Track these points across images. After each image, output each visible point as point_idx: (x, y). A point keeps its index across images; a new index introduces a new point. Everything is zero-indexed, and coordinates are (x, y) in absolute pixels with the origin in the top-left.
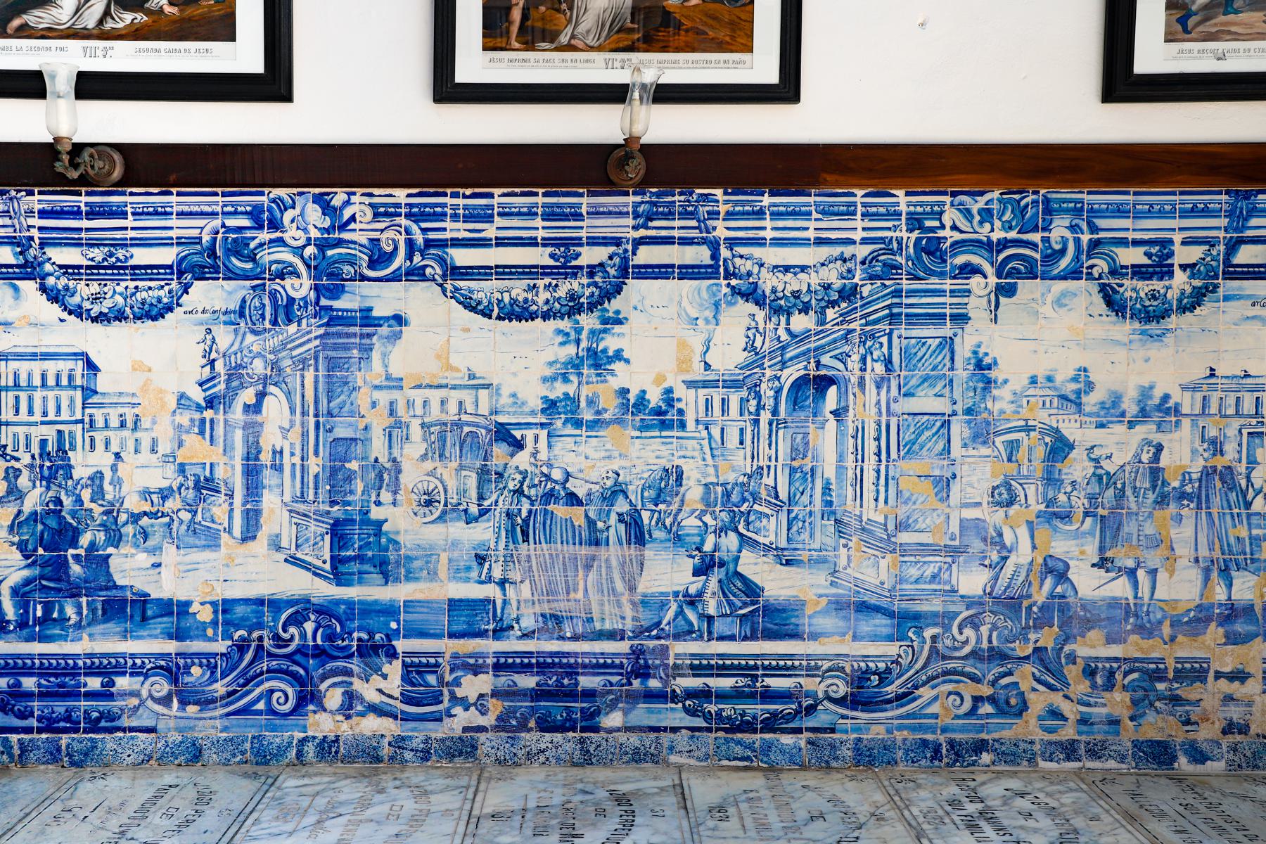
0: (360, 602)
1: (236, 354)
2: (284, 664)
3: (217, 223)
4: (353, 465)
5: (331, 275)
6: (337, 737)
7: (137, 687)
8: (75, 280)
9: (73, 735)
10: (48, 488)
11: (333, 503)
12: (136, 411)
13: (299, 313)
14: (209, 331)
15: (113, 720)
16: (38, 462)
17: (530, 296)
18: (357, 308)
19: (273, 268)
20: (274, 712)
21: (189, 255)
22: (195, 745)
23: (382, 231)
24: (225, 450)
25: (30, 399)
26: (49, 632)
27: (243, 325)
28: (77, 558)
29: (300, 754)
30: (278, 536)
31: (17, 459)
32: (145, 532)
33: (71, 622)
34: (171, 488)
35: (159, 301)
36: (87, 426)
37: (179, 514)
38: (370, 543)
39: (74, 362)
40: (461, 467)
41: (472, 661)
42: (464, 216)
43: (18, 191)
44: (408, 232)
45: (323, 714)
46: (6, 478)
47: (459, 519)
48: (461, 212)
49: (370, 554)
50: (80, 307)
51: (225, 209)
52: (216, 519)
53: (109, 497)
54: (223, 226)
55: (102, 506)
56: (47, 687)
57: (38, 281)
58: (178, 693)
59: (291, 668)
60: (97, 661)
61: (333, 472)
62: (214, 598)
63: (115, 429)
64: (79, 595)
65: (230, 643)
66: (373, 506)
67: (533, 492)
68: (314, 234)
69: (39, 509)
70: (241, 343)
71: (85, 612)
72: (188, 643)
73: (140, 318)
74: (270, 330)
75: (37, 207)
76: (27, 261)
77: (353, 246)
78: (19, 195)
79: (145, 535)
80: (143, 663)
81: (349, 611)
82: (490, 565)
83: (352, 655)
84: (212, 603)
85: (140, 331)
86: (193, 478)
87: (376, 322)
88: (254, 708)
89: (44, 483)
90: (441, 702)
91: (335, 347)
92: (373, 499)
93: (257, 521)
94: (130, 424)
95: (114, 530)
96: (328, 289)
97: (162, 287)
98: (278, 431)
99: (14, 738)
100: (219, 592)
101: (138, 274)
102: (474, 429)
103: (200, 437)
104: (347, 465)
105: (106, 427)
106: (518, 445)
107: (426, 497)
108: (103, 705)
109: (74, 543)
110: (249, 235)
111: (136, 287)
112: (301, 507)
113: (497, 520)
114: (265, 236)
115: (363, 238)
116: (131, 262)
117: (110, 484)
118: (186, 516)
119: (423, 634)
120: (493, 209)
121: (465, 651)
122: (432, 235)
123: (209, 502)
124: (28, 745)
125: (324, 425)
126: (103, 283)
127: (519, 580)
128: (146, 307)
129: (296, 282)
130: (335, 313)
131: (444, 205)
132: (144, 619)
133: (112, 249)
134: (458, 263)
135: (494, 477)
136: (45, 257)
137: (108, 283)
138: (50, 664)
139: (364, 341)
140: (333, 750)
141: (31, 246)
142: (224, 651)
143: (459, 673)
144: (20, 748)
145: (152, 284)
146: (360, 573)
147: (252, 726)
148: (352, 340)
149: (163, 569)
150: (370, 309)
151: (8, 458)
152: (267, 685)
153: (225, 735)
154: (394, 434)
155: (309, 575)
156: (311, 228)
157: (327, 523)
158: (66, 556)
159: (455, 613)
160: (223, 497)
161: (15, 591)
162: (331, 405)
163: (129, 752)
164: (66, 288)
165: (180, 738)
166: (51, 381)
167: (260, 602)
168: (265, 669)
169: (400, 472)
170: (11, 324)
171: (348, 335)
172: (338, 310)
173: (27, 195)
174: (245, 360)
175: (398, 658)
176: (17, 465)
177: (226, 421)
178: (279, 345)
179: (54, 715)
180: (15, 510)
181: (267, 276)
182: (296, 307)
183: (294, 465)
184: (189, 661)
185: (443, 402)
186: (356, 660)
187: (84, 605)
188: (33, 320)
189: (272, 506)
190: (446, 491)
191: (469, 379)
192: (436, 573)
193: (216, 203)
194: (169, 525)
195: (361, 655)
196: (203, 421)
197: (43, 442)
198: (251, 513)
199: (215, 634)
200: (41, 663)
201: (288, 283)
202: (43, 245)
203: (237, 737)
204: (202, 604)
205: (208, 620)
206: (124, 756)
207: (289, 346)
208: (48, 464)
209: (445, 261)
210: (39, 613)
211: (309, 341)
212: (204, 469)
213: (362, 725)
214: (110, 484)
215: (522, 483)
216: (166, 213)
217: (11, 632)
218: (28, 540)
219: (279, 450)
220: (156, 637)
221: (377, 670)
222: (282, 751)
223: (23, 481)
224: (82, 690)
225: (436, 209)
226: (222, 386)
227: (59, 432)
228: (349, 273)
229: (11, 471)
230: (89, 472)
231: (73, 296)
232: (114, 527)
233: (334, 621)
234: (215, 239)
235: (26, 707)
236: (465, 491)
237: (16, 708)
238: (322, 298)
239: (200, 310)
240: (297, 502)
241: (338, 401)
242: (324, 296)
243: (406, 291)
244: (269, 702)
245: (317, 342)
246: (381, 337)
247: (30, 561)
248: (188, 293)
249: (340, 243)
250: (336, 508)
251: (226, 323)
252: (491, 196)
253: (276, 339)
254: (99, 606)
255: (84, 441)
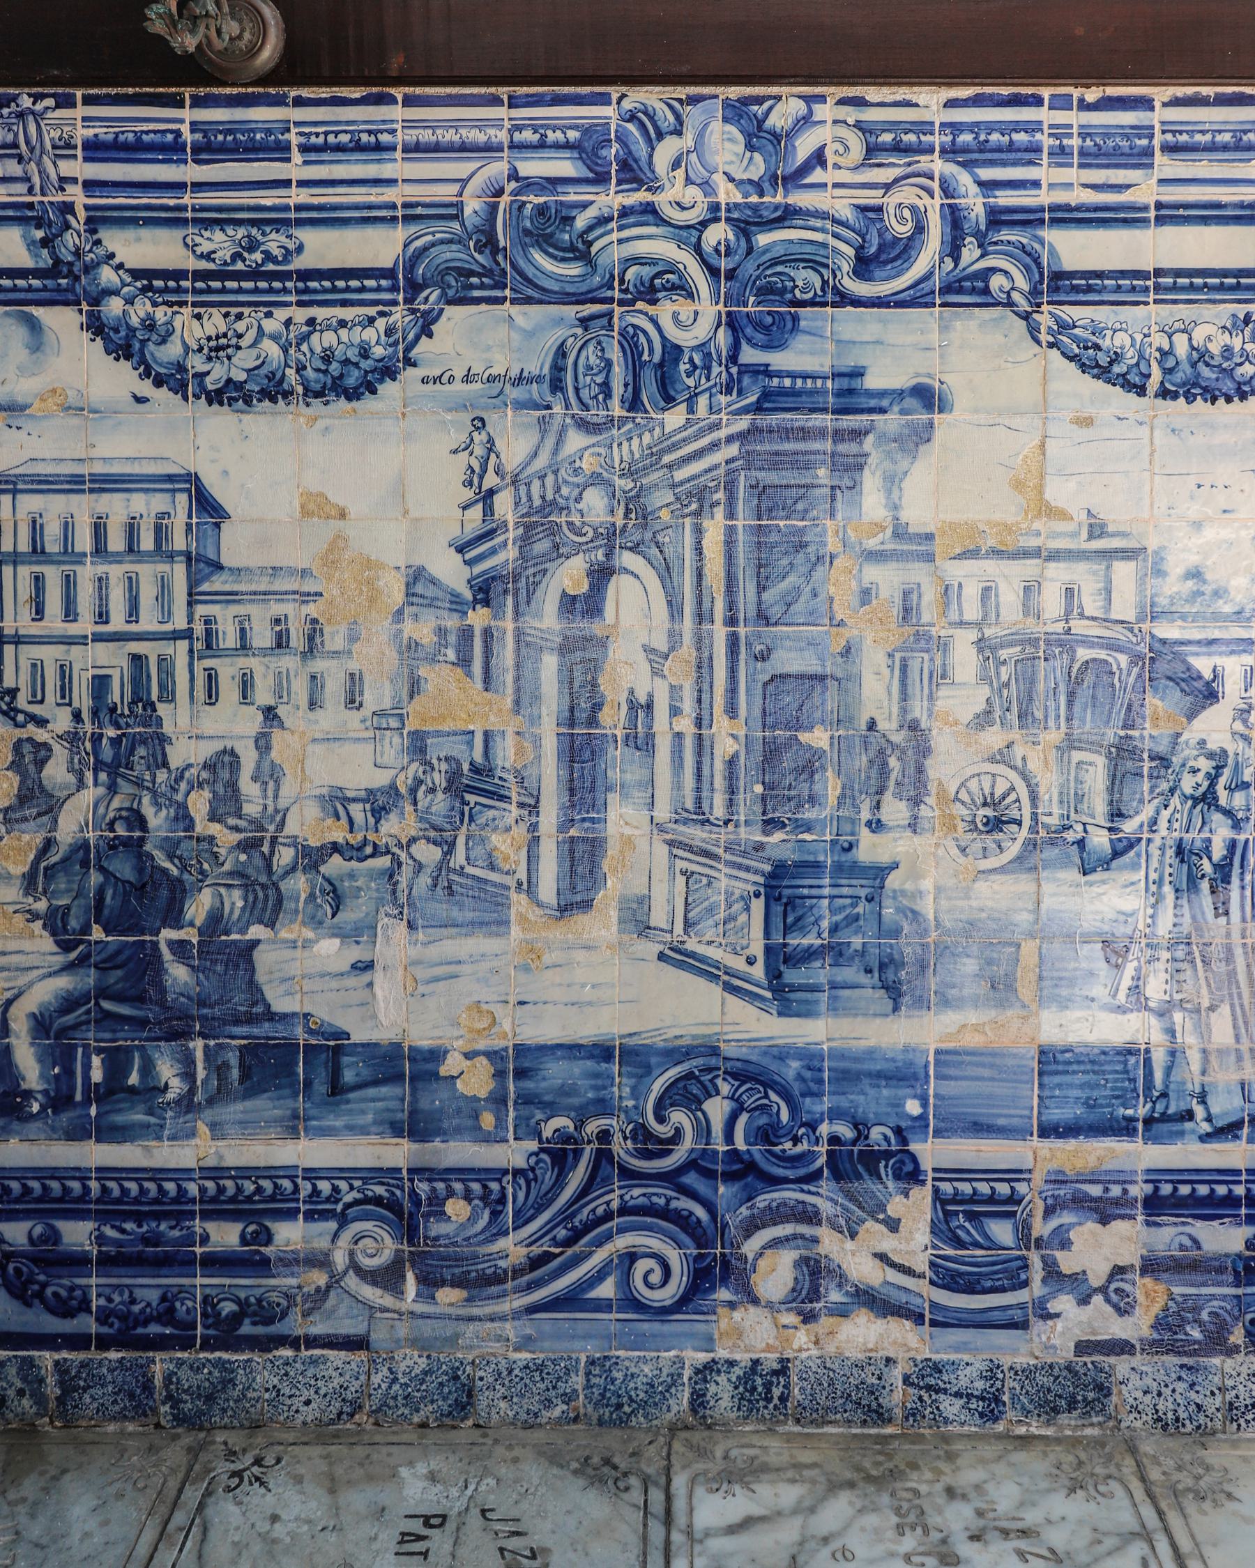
0: (835, 1054)
1: (542, 478)
2: (660, 1195)
3: (498, 168)
4: (818, 738)
5: (766, 292)
6: (784, 1362)
7: (323, 1244)
8: (170, 304)
9: (179, 1355)
10: (112, 789)
11: (771, 824)
12: (311, 609)
13: (691, 382)
14: (480, 423)
15: (269, 1321)
16: (88, 727)
17: (1237, 343)
18: (827, 369)
19: (630, 275)
20: (635, 1304)
21: (433, 245)
22: (456, 1378)
23: (887, 187)
24: (517, 702)
25: (69, 583)
26: (119, 1119)
27: (558, 409)
28: (180, 948)
29: (698, 1401)
30: (644, 901)
31: (41, 722)
32: (335, 891)
33: (170, 1096)
34: (393, 788)
35: (365, 353)
36: (199, 645)
37: (413, 849)
38: (857, 918)
39: (168, 496)
40: (1071, 743)
41: (1095, 1190)
42: (1082, 153)
43: (37, 98)
44: (947, 191)
45: (752, 1309)
46: (16, 766)
47: (1064, 864)
48: (1075, 142)
49: (857, 942)
50: (181, 368)
51: (518, 137)
52: (500, 863)
53: (251, 809)
54: (514, 175)
55: (237, 829)
56: (118, 1243)
57: (85, 307)
58: (417, 1259)
59: (674, 1204)
60: (229, 1184)
61: (771, 753)
62: (499, 1044)
63: (264, 652)
64: (186, 1034)
65: (533, 1145)
66: (865, 833)
67: (1239, 799)
68: (726, 194)
69: (91, 836)
70: (555, 452)
71: (201, 1073)
72: (437, 1144)
73: (318, 395)
74: (623, 421)
75: (82, 133)
76: (57, 262)
77: (818, 223)
78: (39, 107)
79: (336, 896)
80: (336, 1189)
81: (808, 1074)
82: (1138, 969)
83: (815, 1176)
84: (491, 1055)
85: (321, 424)
86: (444, 766)
87: (873, 403)
88: (593, 1294)
89: (103, 776)
90: (1025, 1284)
91: (776, 462)
92: (865, 815)
93: (594, 866)
94: (297, 640)
95: (264, 887)
96: (758, 325)
97: (371, 320)
98: (641, 657)
99: (47, 1358)
100: (507, 1026)
101: (315, 291)
102: (1102, 654)
103: (459, 671)
104: (804, 737)
105: (243, 647)
106: (1210, 694)
107: (989, 812)
108: (245, 1284)
109: (174, 917)
110: (573, 198)
111: (311, 322)
112: (697, 835)
113: (1154, 863)
114: (611, 199)
115: (842, 206)
116: (298, 263)
117: (255, 779)
118: (428, 853)
119: (980, 1128)
120: (1151, 136)
121: (1079, 1164)
122: (1005, 199)
123: (482, 821)
124: (78, 1376)
125: (749, 645)
126: (234, 311)
127: (1206, 1003)
128: (335, 368)
129: (685, 309)
130: (776, 381)
131: (1033, 127)
132: (337, 1089)
133: (254, 231)
134: (1068, 264)
135: (1147, 765)
136: (100, 251)
137: (246, 311)
138: (125, 1191)
139: (843, 448)
140: (777, 1392)
141: (67, 226)
142: (520, 1162)
143: (1067, 1218)
144: (61, 1383)
145: (348, 313)
146: (834, 986)
147: (587, 1337)
148: (816, 445)
149: (378, 976)
150: (858, 373)
151: (20, 718)
152: (622, 1242)
153: (526, 1355)
154: (914, 666)
155: (717, 990)
156: (719, 179)
157: (756, 872)
158: (155, 945)
159: (1057, 1079)
160: (515, 811)
161: (41, 1025)
162: (766, 596)
163: (306, 1394)
164: (149, 324)
165: (423, 1363)
166: (116, 543)
167: (602, 1052)
168: (615, 1205)
169: (925, 751)
170: (23, 408)
171: (805, 434)
172: (780, 374)
173: (58, 106)
174: (565, 491)
175: (923, 1183)
176: (41, 735)
177: (519, 634)
178: (643, 458)
179: (136, 1308)
180: (39, 839)
181: (617, 294)
182: (683, 367)
183: (679, 736)
184: (440, 1186)
185: (1029, 590)
186: (826, 1186)
187: (199, 1055)
188: (72, 398)
189: (628, 831)
190: (1034, 797)
191: (1091, 536)
192: (1011, 987)
193: (497, 123)
194: (391, 875)
195: (838, 1176)
196: (466, 635)
197: (100, 684)
198: (580, 848)
199: (500, 1122)
200: (105, 1190)
201: (665, 310)
202: (93, 224)
203: (554, 1361)
204: (468, 1056)
205: (483, 1094)
206: (297, 1403)
207: (667, 459)
208: (111, 732)
209: (1037, 261)
210: (97, 1075)
211: (715, 445)
212: (470, 744)
213: (842, 1337)
214: (255, 779)
215: (1213, 779)
216: (378, 147)
217: (32, 1117)
218: (68, 907)
219: (643, 700)
220: (364, 1131)
221: (876, 1210)
222: (657, 1394)
223: (57, 772)
224: (198, 1250)
225: (1015, 137)
226: (511, 553)
227: (136, 659)
228: (808, 287)
229: (27, 748)
230: (206, 750)
231: (164, 341)
232: (263, 879)
233: (773, 1096)
234: (494, 208)
235: (72, 1289)
236: (1079, 798)
237: (49, 1291)
238: (745, 346)
239: (459, 373)
240: (686, 822)
241: (783, 585)
242: (749, 341)
243: (944, 328)
244: (625, 1281)
245: (733, 450)
246: (882, 438)
247: (73, 955)
248: (430, 335)
249: (787, 216)
250: (778, 836)
251: (520, 405)
252: (1146, 104)
253: (635, 442)
254: (233, 1058)
255: (192, 679)
